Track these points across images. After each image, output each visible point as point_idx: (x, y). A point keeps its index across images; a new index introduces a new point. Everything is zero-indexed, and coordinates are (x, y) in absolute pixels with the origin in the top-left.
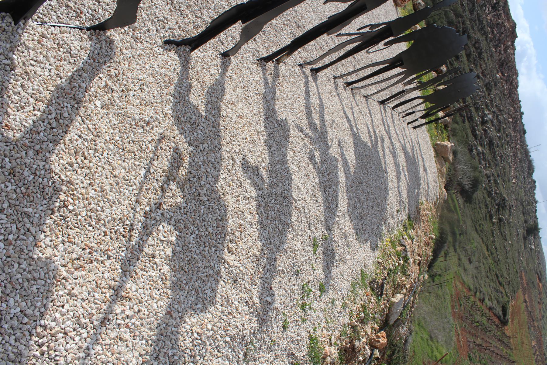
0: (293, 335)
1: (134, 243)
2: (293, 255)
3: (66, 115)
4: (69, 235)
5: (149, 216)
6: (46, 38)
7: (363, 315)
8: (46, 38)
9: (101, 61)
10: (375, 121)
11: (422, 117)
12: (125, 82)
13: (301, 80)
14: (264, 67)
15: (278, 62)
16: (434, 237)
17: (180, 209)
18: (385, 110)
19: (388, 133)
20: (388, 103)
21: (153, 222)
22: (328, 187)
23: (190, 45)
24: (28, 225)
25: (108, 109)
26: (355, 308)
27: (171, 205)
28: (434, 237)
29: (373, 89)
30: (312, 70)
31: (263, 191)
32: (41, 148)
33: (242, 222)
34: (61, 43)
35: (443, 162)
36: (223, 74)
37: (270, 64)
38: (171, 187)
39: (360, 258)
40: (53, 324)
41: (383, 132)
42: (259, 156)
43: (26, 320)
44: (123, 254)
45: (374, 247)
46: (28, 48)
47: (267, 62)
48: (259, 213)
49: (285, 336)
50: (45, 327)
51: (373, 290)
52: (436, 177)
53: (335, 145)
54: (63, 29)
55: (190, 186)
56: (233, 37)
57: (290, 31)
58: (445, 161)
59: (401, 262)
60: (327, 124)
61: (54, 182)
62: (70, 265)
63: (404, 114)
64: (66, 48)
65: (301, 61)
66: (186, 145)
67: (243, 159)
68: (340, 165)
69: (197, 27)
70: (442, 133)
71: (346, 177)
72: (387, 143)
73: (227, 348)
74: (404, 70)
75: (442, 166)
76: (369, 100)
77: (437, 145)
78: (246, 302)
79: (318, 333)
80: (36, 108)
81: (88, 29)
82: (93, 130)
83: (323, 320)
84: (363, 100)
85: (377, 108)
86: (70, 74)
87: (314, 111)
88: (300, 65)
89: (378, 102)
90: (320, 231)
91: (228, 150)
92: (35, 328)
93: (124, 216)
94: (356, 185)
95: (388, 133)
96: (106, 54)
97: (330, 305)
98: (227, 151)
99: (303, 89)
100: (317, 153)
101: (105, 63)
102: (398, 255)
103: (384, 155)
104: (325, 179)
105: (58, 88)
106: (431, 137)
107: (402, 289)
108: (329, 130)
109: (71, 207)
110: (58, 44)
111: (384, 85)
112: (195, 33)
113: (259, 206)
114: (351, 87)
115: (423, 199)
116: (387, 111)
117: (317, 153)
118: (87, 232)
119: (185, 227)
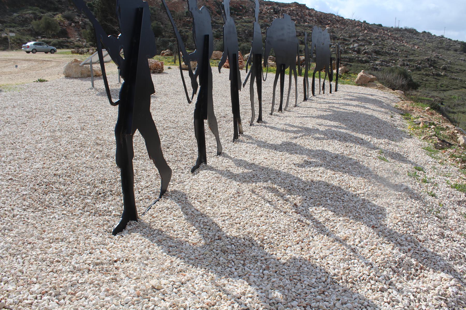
0: (443, 194)
2: (381, 168)
3: (206, 220)
5: (299, 212)
6: (153, 214)
7: (458, 159)
8: (153, 214)
9: (184, 199)
10: (316, 107)
11: (331, 80)
12: (205, 194)
15: (241, 133)
16: (428, 108)
17: (305, 200)
18: (312, 100)
19: (330, 103)
20: (308, 96)
21: (305, 211)
22: (344, 138)
23: (202, 162)
24: (263, 258)
25: (215, 206)
26: (449, 162)
27: (300, 202)
28: (428, 108)
29: (292, 101)
30: (258, 122)
32: (218, 236)
33: (338, 179)
34: (160, 209)
35: (372, 83)
37: (241, 138)
39: (414, 147)
40: (336, 270)
41: (327, 105)
42: (297, 158)
43: (324, 279)
44: (315, 231)
45: (410, 137)
46: (154, 222)
49: (440, 199)
50: (335, 275)
51: (442, 148)
52: (382, 92)
53: (319, 127)
54: (153, 207)
56: (210, 147)
57: (224, 122)
58: (373, 82)
59: (433, 126)
60: (300, 126)
61: (244, 238)
62: (303, 253)
63: (322, 92)
65: (248, 124)
66: (265, 184)
67: (295, 165)
68: (333, 129)
69: (192, 158)
70: (350, 76)
71: (345, 129)
72: (336, 106)
73: (424, 219)
74: (289, 68)
75: (375, 85)
77: (357, 82)
78: (397, 199)
79: (453, 183)
80: (192, 230)
81: (160, 197)
82: (224, 215)
83: (445, 178)
85: (308, 103)
86: (182, 213)
87: (287, 129)
88: (251, 125)
89: (304, 101)
90: (375, 153)
92: (333, 279)
93: (290, 220)
94: (354, 127)
95: (330, 103)
97: (436, 170)
99: (268, 129)
101: (186, 198)
102: (426, 127)
103: (344, 109)
105: (187, 219)
106: (349, 84)
107: (456, 136)
108: (305, 126)
109: (265, 238)
110: (160, 212)
111: (293, 86)
112: (196, 157)
113: (332, 170)
114: (283, 110)
115: (394, 104)
118: (288, 239)
119: (320, 202)
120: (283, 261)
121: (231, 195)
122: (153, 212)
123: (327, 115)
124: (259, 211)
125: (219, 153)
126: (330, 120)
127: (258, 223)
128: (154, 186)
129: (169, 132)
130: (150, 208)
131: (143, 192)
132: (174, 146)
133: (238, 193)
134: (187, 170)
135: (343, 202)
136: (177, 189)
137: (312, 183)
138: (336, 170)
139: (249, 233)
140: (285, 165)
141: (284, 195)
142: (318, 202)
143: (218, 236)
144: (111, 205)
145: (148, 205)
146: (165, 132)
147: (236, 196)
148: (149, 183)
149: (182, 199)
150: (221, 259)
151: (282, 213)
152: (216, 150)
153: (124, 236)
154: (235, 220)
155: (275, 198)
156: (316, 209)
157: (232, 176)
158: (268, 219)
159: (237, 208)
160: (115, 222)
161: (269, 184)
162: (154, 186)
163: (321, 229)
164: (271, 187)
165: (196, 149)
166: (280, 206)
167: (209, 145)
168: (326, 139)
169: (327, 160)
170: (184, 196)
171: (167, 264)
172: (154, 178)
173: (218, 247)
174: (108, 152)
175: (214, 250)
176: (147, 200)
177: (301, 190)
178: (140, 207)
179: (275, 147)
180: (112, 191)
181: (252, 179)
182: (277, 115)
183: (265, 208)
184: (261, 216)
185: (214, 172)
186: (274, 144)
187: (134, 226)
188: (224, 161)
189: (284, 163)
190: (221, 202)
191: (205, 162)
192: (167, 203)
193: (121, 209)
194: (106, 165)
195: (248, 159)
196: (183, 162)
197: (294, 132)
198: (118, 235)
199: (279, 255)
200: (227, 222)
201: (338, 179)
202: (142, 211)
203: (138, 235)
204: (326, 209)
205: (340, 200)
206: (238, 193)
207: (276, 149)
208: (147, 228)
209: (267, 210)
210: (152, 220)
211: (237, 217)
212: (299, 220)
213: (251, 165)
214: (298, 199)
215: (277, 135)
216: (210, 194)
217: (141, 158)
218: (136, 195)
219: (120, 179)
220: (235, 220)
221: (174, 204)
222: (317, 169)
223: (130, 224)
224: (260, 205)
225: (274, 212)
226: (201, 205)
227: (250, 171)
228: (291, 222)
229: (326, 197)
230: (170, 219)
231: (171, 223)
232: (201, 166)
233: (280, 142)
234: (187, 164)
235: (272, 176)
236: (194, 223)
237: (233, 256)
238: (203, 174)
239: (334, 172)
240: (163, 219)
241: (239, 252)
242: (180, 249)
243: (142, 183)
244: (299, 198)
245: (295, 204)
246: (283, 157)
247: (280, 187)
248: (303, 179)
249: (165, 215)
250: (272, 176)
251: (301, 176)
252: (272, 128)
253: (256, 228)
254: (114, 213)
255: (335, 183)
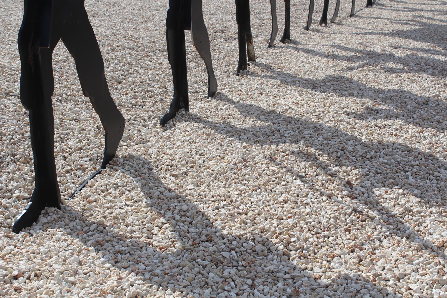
1: (378, 217)
3: (185, 207)
4: (326, 255)
5: (355, 196)
6: (89, 196)
8: (89, 196)
9: (146, 171)
10: (389, 16)
12: (184, 162)
13: (288, 52)
14: (250, 73)
15: (252, 59)
17: (367, 175)
18: (383, 5)
21: (366, 195)
24: (288, 276)
25: (203, 183)
27: (357, 179)
30: (283, 41)
31: (402, 114)
32: (207, 236)
33: (428, 141)
34: (103, 188)
36: (232, 102)
37: (251, 68)
38: (334, 169)
41: (410, 14)
42: (353, 104)
44: (384, 229)
46: (90, 209)
47: (246, 68)
48: (428, 126)
53: (393, 51)
54: (89, 183)
55: (346, 159)
56: (196, 82)
57: (222, 40)
60: (359, 48)
61: (254, 240)
64: (111, 187)
67: (348, 114)
69: (163, 101)
71: (443, 55)
72: (426, 15)
76: (358, 14)
80: (160, 224)
81: (104, 167)
82: (218, 198)
84: (353, 19)
85: (374, 11)
86: (142, 194)
87: (336, 53)
88: (270, 46)
91: (327, 120)
93: (338, 209)
96: (140, 165)
98: (328, 122)
99: (301, 53)
100: (391, 65)
101: (150, 169)
104: (431, 70)
105: (152, 206)
108: (369, 49)
109: (293, 239)
110: (103, 192)
112: (170, 99)
114: (328, 21)
116: (384, 3)
117: (391, 65)
119: (394, 179)
120: (324, 281)
121: (232, 165)
122: (89, 193)
123: (410, 31)
124: (282, 193)
125: (212, 94)
126: (415, 39)
127: (280, 213)
128: (93, 148)
129: (122, 56)
130: (84, 186)
131: (73, 157)
132: (130, 79)
133: (245, 161)
134: (153, 122)
135: (437, 180)
136: (133, 153)
137: (380, 147)
138: (425, 126)
139: (263, 230)
140: (331, 114)
141: (327, 166)
142: (391, 180)
143: (207, 236)
144: (12, 179)
145: (81, 180)
146: (114, 54)
147: (240, 166)
148: (84, 143)
149: (143, 171)
150: (211, 275)
151: (324, 198)
152: (205, 88)
153: (35, 235)
154: (238, 208)
155: (311, 172)
156: (386, 192)
157: (235, 133)
158: (298, 207)
159: (243, 187)
160: (18, 209)
161: (301, 146)
162: (93, 148)
163: (395, 226)
164: (305, 151)
165: (171, 87)
166: (319, 184)
167: (193, 79)
168: (407, 72)
169: (409, 107)
170: (146, 166)
171: (112, 282)
172: (93, 133)
173: (206, 254)
174: (9, 86)
175: (199, 260)
176: (79, 173)
177: (359, 159)
178: (66, 184)
179: (313, 85)
180: (14, 155)
181: (271, 138)
182: (318, 31)
183: (293, 188)
184: (286, 202)
185: (201, 125)
186: (311, 80)
187: (54, 216)
188: (219, 108)
189: (329, 112)
190: (213, 176)
191: (187, 107)
192: (117, 177)
193: (30, 187)
194: (5, 110)
195: (263, 104)
196: (147, 108)
197: (349, 59)
198: (23, 233)
199: (318, 271)
200: (223, 211)
201: (428, 141)
202: (70, 191)
203: (59, 233)
204: (406, 191)
205: (431, 177)
206: (245, 161)
207: (314, 88)
208: (77, 221)
209: (296, 192)
210: (86, 207)
211: (242, 203)
212: (355, 210)
213: (269, 115)
214: (353, 174)
215: (317, 64)
216: (194, 163)
217: (69, 98)
218: (59, 162)
219: (28, 134)
220: (238, 208)
221: (129, 178)
222: (390, 122)
223: (47, 213)
224: (284, 183)
225: (310, 196)
226: (177, 182)
227: (267, 124)
228: (340, 214)
229: (405, 172)
230: (119, 204)
231: (122, 211)
232: (179, 115)
233: (321, 76)
234: (152, 111)
235: (306, 133)
236: (163, 212)
237: (233, 271)
238: (181, 129)
239: (420, 129)
240: (107, 205)
241: (244, 263)
242: (136, 257)
243: (70, 143)
244: (356, 171)
245: (349, 183)
246: (327, 101)
247: (321, 152)
248: (364, 138)
249: (111, 198)
250: (307, 132)
251: (361, 134)
252: (308, 51)
253: (275, 222)
254: (17, 193)
255: (423, 147)
